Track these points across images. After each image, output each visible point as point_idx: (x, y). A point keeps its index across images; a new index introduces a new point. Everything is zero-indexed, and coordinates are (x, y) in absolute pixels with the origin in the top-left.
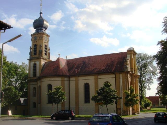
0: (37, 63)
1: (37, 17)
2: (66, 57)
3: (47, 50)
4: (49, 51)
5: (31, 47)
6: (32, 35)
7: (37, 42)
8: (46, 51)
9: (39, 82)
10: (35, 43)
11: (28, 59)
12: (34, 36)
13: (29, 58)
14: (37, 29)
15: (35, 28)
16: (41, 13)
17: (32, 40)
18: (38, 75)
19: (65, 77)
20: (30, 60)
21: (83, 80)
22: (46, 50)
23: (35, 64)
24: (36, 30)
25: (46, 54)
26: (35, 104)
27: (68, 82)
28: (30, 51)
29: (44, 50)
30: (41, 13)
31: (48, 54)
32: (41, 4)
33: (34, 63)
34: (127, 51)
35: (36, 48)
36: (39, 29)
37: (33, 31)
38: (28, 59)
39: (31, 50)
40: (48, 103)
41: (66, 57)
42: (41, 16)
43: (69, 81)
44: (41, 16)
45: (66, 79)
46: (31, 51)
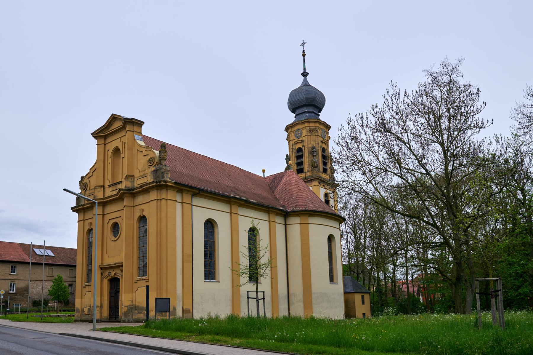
3: (328, 161)
5: (287, 156)
6: (287, 129)
7: (302, 141)
10: (300, 145)
12: (295, 129)
14: (298, 111)
15: (293, 111)
16: (305, 74)
17: (288, 139)
30: (305, 74)
31: (329, 172)
32: (304, 51)
37: (291, 118)
42: (306, 84)
44: (306, 84)
46: (288, 165)
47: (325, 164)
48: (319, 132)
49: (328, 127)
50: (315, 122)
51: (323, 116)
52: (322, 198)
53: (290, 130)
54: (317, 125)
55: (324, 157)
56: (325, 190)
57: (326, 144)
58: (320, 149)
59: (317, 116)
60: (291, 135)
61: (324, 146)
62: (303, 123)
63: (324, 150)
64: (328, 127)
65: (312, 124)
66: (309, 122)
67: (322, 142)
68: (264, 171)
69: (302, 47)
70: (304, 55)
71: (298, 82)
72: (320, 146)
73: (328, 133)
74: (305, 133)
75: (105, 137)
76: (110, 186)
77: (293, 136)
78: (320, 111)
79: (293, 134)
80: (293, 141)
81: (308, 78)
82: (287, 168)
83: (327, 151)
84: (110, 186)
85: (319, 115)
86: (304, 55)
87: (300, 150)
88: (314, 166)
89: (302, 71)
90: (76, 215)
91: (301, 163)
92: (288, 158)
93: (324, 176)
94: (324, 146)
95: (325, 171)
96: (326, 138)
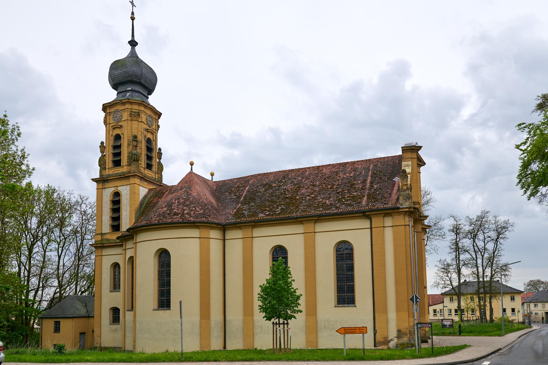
0: (125, 190)
2: (212, 175)
3: (154, 155)
4: (160, 159)
7: (121, 126)
8: (149, 158)
9: (129, 245)
11: (93, 180)
12: (113, 110)
13: (97, 176)
14: (121, 89)
15: (115, 87)
16: (133, 43)
18: (126, 223)
19: (212, 228)
20: (102, 181)
21: (265, 240)
22: (149, 154)
23: (117, 194)
24: (118, 94)
25: (149, 167)
26: (115, 311)
27: (220, 243)
29: (144, 152)
30: (133, 43)
31: (155, 168)
32: (133, 13)
33: (113, 189)
34: (400, 153)
35: (119, 147)
36: (128, 89)
37: (111, 95)
38: (93, 180)
39: (102, 152)
40: (156, 307)
41: (212, 175)
42: (133, 55)
43: (224, 240)
44: (133, 55)
45: (215, 234)
47: (149, 158)
48: (143, 117)
49: (159, 115)
50: (140, 104)
51: (153, 100)
54: (142, 108)
55: (149, 149)
59: (145, 98)
60: (108, 117)
61: (149, 136)
62: (124, 104)
64: (159, 115)
65: (135, 107)
66: (131, 103)
67: (147, 130)
70: (133, 19)
71: (124, 52)
74: (126, 116)
77: (111, 120)
78: (150, 91)
79: (111, 117)
81: (137, 48)
83: (154, 143)
85: (148, 98)
86: (133, 19)
88: (134, 159)
89: (130, 39)
91: (119, 154)
92: (102, 146)
93: (147, 172)
95: (149, 167)
96: (154, 127)
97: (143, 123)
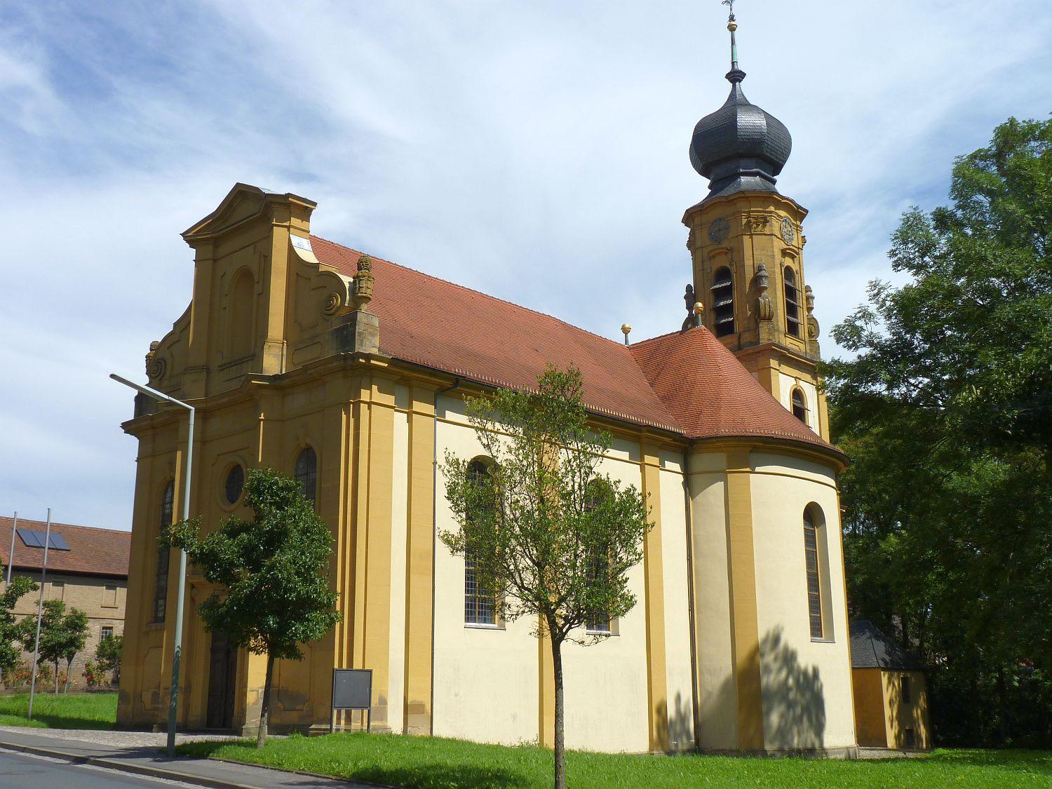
1: (714, 99)
3: (801, 302)
4: (810, 309)
5: (689, 287)
6: (691, 217)
8: (791, 310)
10: (722, 261)
15: (704, 172)
16: (735, 76)
17: (691, 245)
25: (793, 329)
28: (686, 314)
30: (735, 76)
31: (803, 331)
32: (732, 18)
37: (698, 188)
46: (690, 314)
47: (791, 310)
51: (786, 184)
52: (786, 402)
53: (697, 220)
55: (790, 292)
56: (793, 381)
57: (793, 257)
58: (778, 270)
60: (698, 234)
63: (789, 274)
68: (626, 331)
69: (727, 7)
70: (732, 29)
72: (777, 262)
73: (799, 229)
75: (216, 242)
76: (223, 368)
78: (777, 169)
80: (706, 251)
81: (745, 86)
82: (691, 322)
84: (223, 368)
85: (774, 182)
86: (732, 29)
87: (723, 274)
89: (729, 69)
90: (133, 442)
92: (691, 297)
93: (789, 342)
94: (788, 262)
95: (793, 329)
97: (774, 238)
